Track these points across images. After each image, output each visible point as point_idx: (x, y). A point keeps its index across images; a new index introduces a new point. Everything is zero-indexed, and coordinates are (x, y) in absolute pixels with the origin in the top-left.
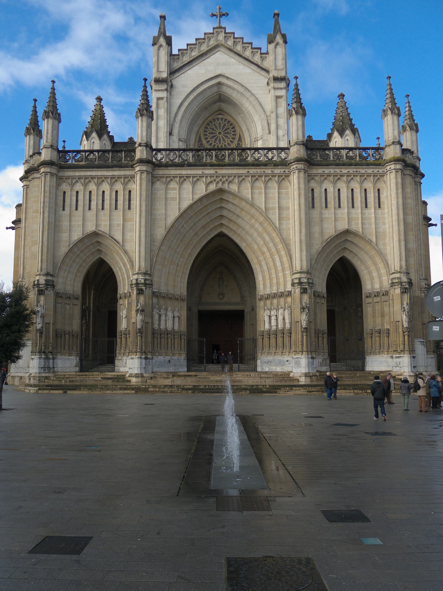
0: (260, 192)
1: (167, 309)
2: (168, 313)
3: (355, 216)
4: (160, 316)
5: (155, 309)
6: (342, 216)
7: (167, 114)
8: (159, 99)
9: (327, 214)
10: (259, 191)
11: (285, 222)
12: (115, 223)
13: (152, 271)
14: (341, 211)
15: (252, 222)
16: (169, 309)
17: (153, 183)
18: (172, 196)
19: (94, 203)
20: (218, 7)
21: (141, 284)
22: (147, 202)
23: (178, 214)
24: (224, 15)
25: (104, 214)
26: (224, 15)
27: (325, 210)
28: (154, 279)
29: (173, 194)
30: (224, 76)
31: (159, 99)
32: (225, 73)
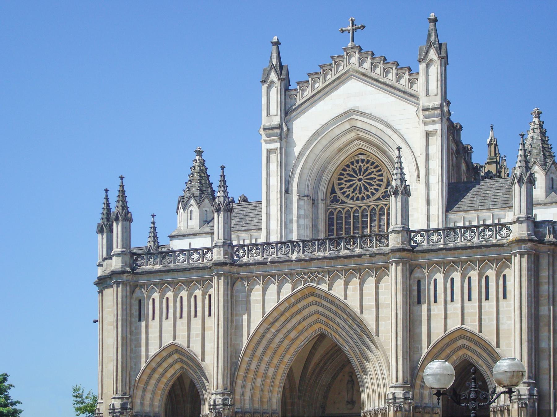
0: (355, 287)
3: (472, 311)
6: (455, 312)
7: (281, 169)
8: (269, 152)
9: (436, 311)
10: (353, 286)
11: (384, 322)
12: (194, 333)
14: (454, 305)
17: (233, 285)
18: (255, 299)
19: (171, 311)
21: (219, 405)
22: (226, 309)
23: (261, 319)
25: (182, 323)
27: (433, 305)
29: (256, 294)
30: (358, 111)
31: (269, 152)
32: (358, 107)
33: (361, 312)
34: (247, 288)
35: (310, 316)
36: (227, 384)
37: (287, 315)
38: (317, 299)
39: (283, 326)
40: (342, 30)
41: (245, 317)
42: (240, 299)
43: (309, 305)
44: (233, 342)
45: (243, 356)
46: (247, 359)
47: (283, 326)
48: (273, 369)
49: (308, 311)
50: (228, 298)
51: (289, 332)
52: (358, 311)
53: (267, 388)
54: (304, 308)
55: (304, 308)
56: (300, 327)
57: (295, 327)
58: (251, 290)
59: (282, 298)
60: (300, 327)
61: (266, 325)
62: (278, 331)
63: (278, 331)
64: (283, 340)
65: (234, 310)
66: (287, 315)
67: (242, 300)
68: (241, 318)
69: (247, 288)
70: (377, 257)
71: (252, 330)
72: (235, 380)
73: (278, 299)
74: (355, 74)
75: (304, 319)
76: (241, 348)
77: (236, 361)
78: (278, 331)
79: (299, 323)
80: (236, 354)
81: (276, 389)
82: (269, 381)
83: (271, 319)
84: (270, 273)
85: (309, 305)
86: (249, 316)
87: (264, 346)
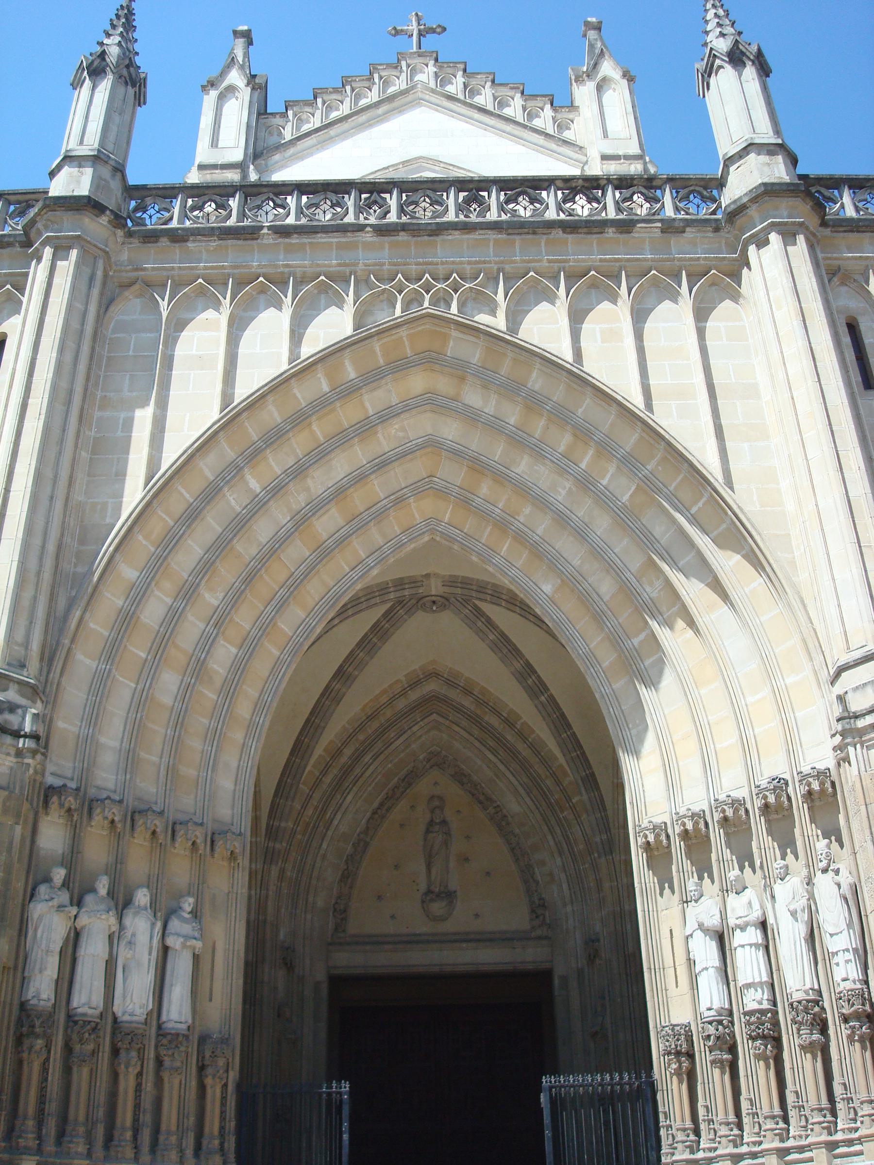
1: (128, 902)
2: (128, 921)
4: (75, 937)
5: (43, 889)
13: (55, 675)
15: (583, 465)
16: (142, 897)
17: (107, 304)
18: (194, 352)
20: (413, 14)
23: (216, 416)
24: (432, 31)
26: (432, 31)
28: (60, 724)
33: (649, 406)
34: (165, 314)
35: (404, 455)
36: (26, 645)
37: (319, 430)
38: (443, 384)
39: (299, 472)
40: (395, 28)
41: (144, 417)
42: (131, 353)
43: (407, 407)
44: (78, 496)
45: (116, 549)
46: (128, 572)
47: (299, 472)
48: (234, 650)
49: (401, 434)
50: (72, 382)
51: (317, 507)
52: (636, 400)
53: (199, 721)
54: (387, 415)
55: (387, 415)
56: (359, 500)
57: (339, 493)
58: (179, 325)
59: (308, 350)
60: (359, 500)
61: (227, 451)
62: (276, 490)
63: (276, 490)
64: (288, 536)
65: (97, 384)
66: (319, 430)
67: (135, 356)
68: (123, 415)
69: (165, 314)
70: (690, 233)
71: (171, 455)
72: (67, 642)
73: (294, 355)
74: (427, 97)
75: (382, 464)
76: (108, 520)
77: (80, 570)
78: (273, 489)
79: (359, 478)
80: (82, 541)
81: (238, 736)
82: (209, 695)
83: (252, 430)
84: (264, 270)
85: (407, 407)
86: (162, 405)
87: (210, 538)
